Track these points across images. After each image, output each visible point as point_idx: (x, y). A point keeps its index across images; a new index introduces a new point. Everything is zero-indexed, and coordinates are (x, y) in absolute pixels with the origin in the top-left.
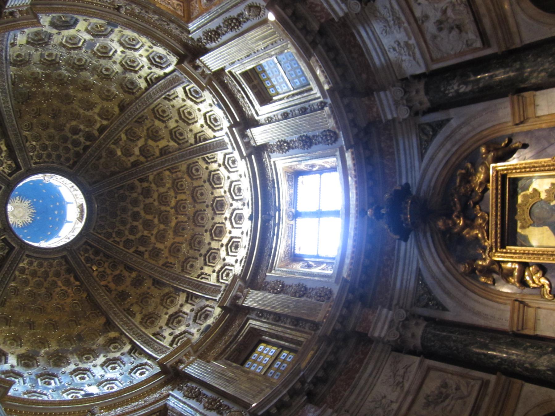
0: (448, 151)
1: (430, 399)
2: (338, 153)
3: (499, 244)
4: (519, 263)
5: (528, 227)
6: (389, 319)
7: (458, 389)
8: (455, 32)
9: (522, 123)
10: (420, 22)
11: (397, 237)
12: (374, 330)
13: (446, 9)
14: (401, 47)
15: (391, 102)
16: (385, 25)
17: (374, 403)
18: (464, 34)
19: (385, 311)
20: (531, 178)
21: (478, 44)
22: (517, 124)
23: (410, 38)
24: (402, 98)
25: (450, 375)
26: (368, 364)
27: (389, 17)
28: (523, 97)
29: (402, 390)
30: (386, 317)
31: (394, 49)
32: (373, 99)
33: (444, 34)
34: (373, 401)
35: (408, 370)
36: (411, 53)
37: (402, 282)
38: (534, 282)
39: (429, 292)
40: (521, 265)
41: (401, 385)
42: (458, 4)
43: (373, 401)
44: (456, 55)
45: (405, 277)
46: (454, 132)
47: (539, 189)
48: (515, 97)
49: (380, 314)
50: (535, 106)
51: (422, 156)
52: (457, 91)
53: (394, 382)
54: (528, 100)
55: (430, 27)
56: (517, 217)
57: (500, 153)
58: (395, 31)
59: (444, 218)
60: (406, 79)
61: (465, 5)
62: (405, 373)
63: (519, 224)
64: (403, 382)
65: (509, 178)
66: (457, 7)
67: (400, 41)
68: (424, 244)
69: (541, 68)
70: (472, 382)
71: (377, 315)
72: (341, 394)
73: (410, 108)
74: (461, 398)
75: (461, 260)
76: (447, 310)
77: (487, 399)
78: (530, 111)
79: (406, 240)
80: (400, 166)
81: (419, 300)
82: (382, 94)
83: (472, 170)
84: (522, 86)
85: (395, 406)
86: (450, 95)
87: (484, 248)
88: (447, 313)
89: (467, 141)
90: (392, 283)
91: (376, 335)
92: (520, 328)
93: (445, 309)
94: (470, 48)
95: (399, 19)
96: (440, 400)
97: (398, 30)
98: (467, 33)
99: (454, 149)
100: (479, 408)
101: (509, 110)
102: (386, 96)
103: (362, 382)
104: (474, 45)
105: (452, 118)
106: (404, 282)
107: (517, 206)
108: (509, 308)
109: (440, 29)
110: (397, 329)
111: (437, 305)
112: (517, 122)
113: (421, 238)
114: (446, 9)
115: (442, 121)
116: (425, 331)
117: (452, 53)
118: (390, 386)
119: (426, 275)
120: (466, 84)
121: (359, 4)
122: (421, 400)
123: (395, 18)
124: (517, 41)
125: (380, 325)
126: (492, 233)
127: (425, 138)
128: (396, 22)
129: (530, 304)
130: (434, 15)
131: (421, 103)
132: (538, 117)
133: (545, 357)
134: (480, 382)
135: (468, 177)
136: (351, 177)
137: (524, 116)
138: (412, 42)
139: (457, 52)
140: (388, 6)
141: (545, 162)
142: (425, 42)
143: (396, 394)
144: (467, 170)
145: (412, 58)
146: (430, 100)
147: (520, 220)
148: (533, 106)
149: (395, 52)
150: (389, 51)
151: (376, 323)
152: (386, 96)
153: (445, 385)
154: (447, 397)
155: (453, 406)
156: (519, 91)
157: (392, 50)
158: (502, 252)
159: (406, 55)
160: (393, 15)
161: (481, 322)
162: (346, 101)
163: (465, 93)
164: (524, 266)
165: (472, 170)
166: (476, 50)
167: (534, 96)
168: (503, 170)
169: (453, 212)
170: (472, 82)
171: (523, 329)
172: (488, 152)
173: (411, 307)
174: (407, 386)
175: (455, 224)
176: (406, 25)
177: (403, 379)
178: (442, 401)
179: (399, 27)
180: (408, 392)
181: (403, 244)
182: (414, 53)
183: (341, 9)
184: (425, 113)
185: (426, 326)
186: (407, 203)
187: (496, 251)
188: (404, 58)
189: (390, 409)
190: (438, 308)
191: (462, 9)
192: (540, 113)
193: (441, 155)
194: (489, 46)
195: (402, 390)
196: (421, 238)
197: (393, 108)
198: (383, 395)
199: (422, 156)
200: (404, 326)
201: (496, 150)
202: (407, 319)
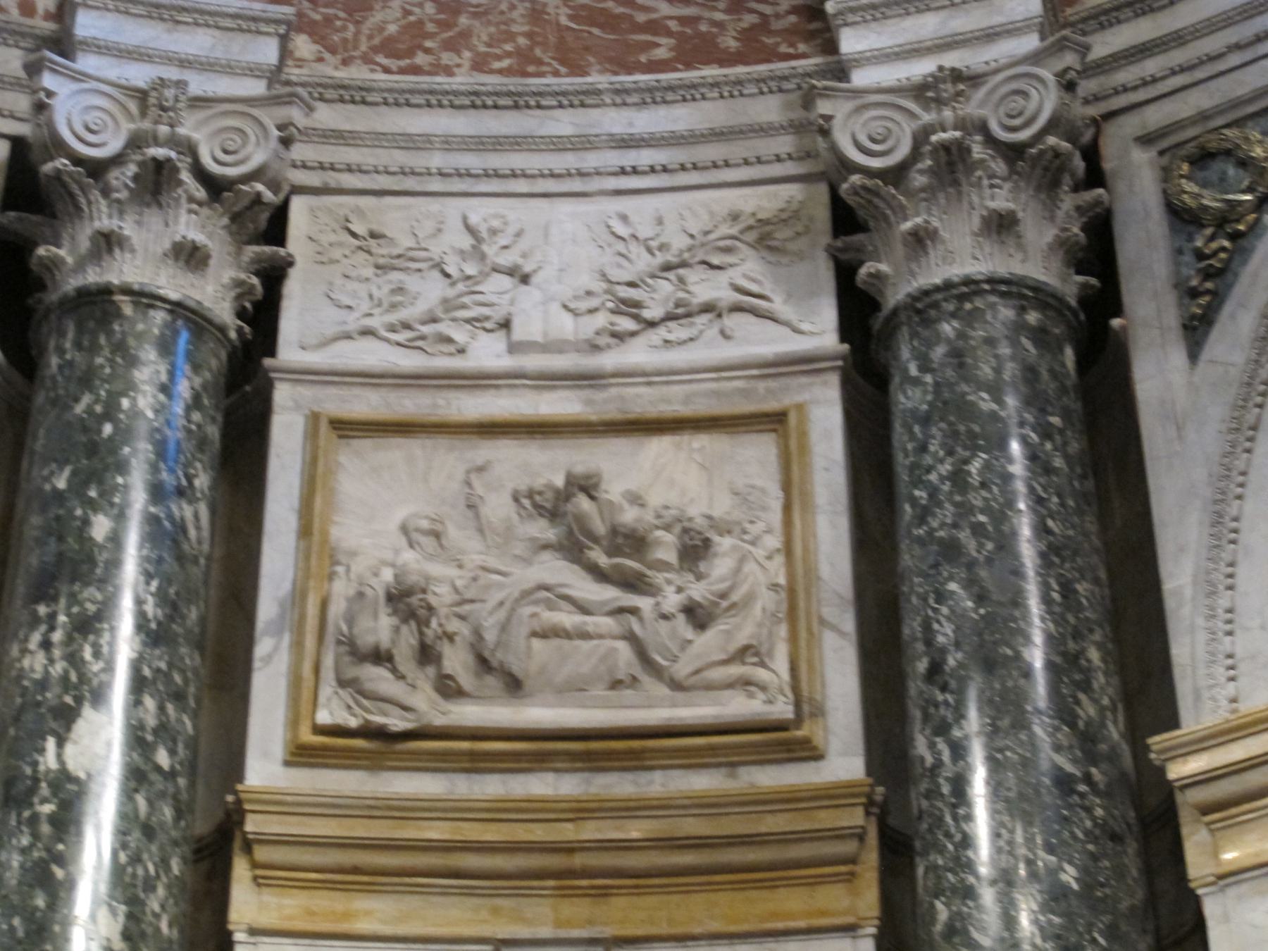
7: (698, 616)
17: (466, 242)
25: (774, 542)
26: (689, 93)
29: (595, 348)
34: (471, 230)
35: (733, 322)
41: (627, 324)
43: (471, 230)
53: (632, 284)
62: (708, 308)
64: (652, 324)
72: (447, 58)
76: (1194, 355)
81: (1203, 158)
88: (1178, 356)
96: (600, 557)
100: (635, 762)
103: (563, 123)
111: (1208, 274)
118: (604, 276)
134: (783, 709)
143: (566, 326)
154: (633, 583)
155: (585, 636)
171: (1206, 809)
174: (638, 354)
177: (670, 317)
178: (600, 575)
189: (460, 335)
190: (1194, 293)
198: (527, 268)
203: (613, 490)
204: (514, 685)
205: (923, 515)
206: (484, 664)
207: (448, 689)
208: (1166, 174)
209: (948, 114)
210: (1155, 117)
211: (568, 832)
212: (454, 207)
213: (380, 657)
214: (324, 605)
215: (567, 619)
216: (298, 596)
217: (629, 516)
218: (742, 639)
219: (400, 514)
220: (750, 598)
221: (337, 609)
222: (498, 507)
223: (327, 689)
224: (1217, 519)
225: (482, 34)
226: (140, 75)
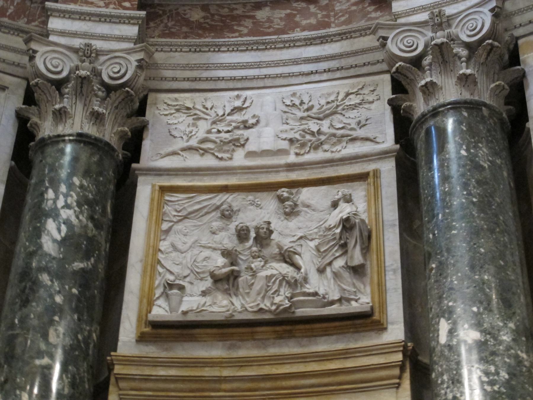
10: (284, 192)
16: (315, 110)
23: (250, 154)
24: (97, 74)
27: (332, 126)
36: (205, 146)
58: (286, 127)
86: (51, 194)
94: (158, 293)
95: (316, 148)
97: (284, 136)
98: (204, 293)
117: (164, 245)
123: (323, 138)
128: (308, 137)
139: (160, 256)
140: (361, 133)
142: (225, 189)
145: (193, 142)
149: (228, 111)
163: (38, 232)
176: (292, 159)
179: (291, 141)
194: (142, 339)
197: (77, 43)
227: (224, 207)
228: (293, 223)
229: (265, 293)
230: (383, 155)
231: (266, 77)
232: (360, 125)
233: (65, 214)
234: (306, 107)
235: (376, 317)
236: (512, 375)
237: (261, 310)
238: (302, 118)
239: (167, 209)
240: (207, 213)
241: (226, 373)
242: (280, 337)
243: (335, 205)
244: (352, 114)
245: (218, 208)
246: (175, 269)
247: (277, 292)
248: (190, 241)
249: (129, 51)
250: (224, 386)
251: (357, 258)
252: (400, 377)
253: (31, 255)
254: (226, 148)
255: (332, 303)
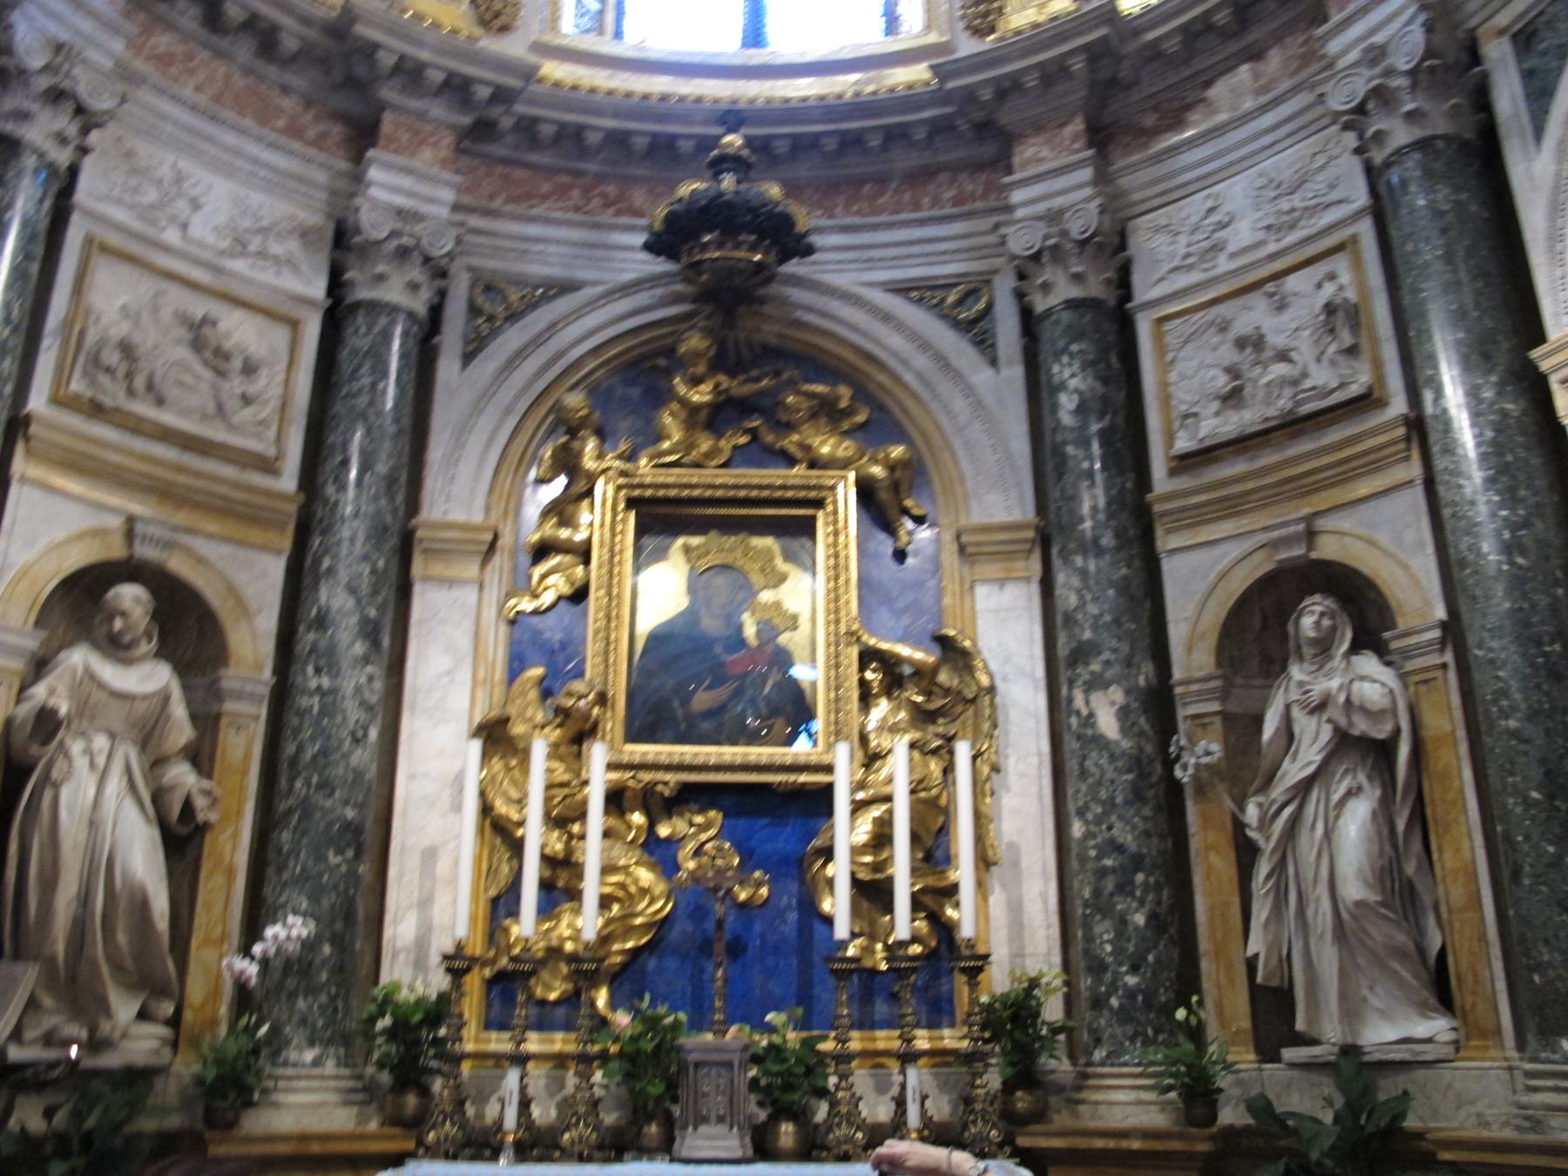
0: (905, 362)
1: (207, 331)
2: (933, 38)
3: (637, 493)
4: (589, 541)
5: (689, 561)
6: (425, 208)
7: (247, 400)
8: (1222, 382)
9: (962, 549)
10: (1270, 287)
11: (658, 226)
12: (388, 166)
13: (1290, 361)
14: (1214, 231)
15: (1057, 202)
18: (1215, 405)
19: (448, 195)
20: (812, 569)
21: (1183, 444)
22: (958, 536)
23: (1233, 256)
24: (1064, 233)
25: (281, 378)
28: (1030, 551)
30: (430, 200)
31: (1211, 210)
32: (1076, 146)
33: (1228, 354)
36: (1191, 260)
37: (538, 240)
38: (544, 576)
39: (513, 317)
40: (584, 548)
41: (238, 249)
42: (1295, 396)
44: (1164, 385)
45: (552, 249)
46: (957, 376)
47: (784, 587)
48: (1030, 534)
49: (435, 181)
50: (1002, 582)
51: (902, 289)
52: (1062, 386)
54: (1020, 564)
55: (1254, 315)
56: (713, 534)
57: (884, 495)
59: (712, 353)
60: (1123, 246)
61: (1290, 412)
63: (695, 541)
65: (813, 519)
66: (1288, 392)
67: (1228, 229)
68: (643, 298)
69: (1089, 597)
70: (272, 432)
71: (435, 170)
73: (1036, 257)
74: (220, 408)
75: (599, 395)
77: (228, 471)
78: (993, 569)
79: (648, 247)
80: (875, 227)
81: (488, 288)
82: (1087, 173)
83: (846, 426)
84: (1055, 550)
85: (172, 236)
86: (1056, 369)
87: (631, 457)
88: (457, 365)
89: (929, 412)
90: (535, 211)
91: (374, 173)
92: (426, 545)
93: (468, 358)
94: (1177, 424)
95: (1292, 226)
98: (1217, 414)
99: (908, 377)
101: (1000, 517)
102: (1079, 187)
103: (231, 139)
104: (1181, 434)
105: (998, 371)
106: (539, 247)
107: (741, 537)
108: (477, 517)
109: (1241, 343)
110: (394, 234)
112: (964, 539)
113: (659, 292)
114: (1290, 361)
115: (993, 346)
116: (393, 309)
117: (1173, 376)
119: (561, 306)
120: (1081, 410)
121: (1348, 107)
122: (199, 307)
124: (1175, 541)
125: (407, 182)
126: (672, 476)
127: (951, 299)
128: (1285, 218)
129: (490, 567)
130: (1277, 329)
131: (1046, 287)
132: (972, 588)
133: (351, 603)
134: (271, 452)
135: (828, 413)
136: (855, 83)
137: (982, 554)
138: (1223, 265)
140: (1334, 196)
141: (847, 603)
142: (1214, 302)
143: (210, 239)
144: (848, 413)
145: (1176, 262)
146: (1049, 312)
147: (704, 545)
148: (1002, 575)
150: (1208, 196)
151: (408, 171)
152: (1079, 187)
153: (249, 369)
154: (221, 374)
156: (1044, 542)
157: (1210, 204)
158: (615, 500)
159: (1189, 245)
160: (1306, 209)
161: (436, 453)
162: (1077, 64)
163: (1055, 407)
164: (584, 553)
165: (846, 426)
166: (1170, 438)
167: (1027, 579)
168: (835, 502)
169: (732, 374)
170: (1084, 427)
172: (892, 467)
173: (470, 269)
174: (239, 265)
175: (695, 381)
176: (1272, 247)
178: (206, 363)
179: (1268, 228)
180: (217, 270)
181: (640, 239)
182: (1190, 267)
183: (1344, 52)
184: (1020, 295)
185: (411, 315)
186: (753, 248)
187: (619, 488)
188: (1183, 240)
191: (1281, 403)
192: (981, 591)
193: (896, 341)
194: (1173, 472)
195: (222, 253)
196: (659, 292)
197: (1041, 207)
199: (902, 289)
200: (403, 254)
201: (896, 486)
202: (427, 260)
203: (223, 326)
204: (160, 402)
205: (354, 396)
206: (150, 387)
207: (131, 393)
208: (473, 286)
209: (408, 228)
210: (477, 262)
211: (170, 476)
212: (170, 158)
213: (109, 370)
214: (82, 333)
215: (188, 379)
216: (68, 323)
217: (228, 345)
218: (262, 416)
219: (120, 302)
220: (269, 400)
221: (91, 338)
222: (166, 314)
223: (77, 375)
224: (458, 440)
225: (201, 76)
226: (64, 36)
227: (1218, 321)
228: (1286, 317)
229: (1268, 401)
230: (1356, 216)
231: (1232, 164)
232: (1332, 187)
233: (1074, 383)
234: (1274, 185)
235: (1376, 395)
236: (1498, 431)
237: (1267, 419)
238: (1275, 198)
239: (1168, 339)
240: (1204, 332)
241: (1250, 485)
242: (1295, 436)
243: (1319, 286)
244: (1321, 177)
245: (1212, 323)
246: (1188, 397)
247: (1278, 397)
248: (1195, 363)
249: (1088, 200)
250: (1254, 497)
251: (1347, 339)
252: (1408, 449)
253: (1055, 430)
254: (1209, 256)
255: (1333, 391)
